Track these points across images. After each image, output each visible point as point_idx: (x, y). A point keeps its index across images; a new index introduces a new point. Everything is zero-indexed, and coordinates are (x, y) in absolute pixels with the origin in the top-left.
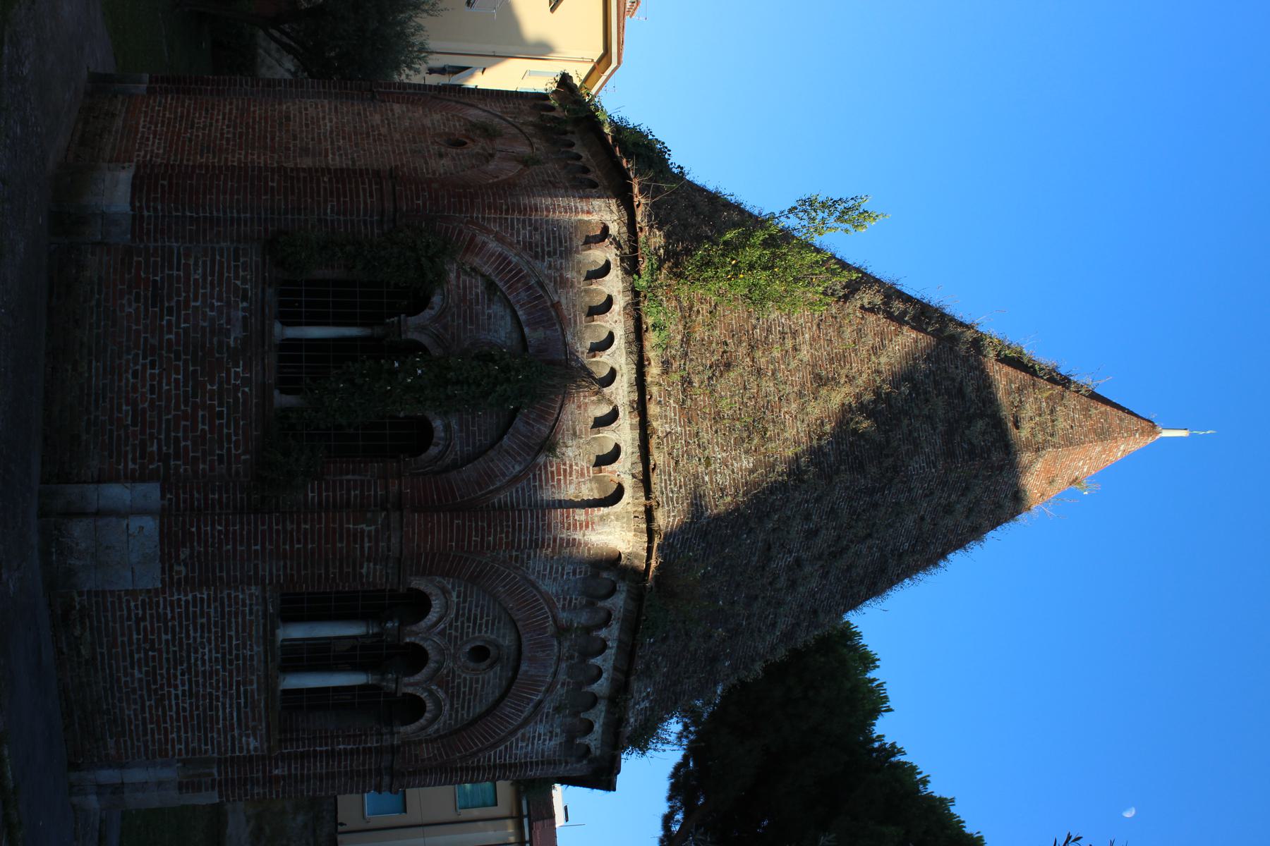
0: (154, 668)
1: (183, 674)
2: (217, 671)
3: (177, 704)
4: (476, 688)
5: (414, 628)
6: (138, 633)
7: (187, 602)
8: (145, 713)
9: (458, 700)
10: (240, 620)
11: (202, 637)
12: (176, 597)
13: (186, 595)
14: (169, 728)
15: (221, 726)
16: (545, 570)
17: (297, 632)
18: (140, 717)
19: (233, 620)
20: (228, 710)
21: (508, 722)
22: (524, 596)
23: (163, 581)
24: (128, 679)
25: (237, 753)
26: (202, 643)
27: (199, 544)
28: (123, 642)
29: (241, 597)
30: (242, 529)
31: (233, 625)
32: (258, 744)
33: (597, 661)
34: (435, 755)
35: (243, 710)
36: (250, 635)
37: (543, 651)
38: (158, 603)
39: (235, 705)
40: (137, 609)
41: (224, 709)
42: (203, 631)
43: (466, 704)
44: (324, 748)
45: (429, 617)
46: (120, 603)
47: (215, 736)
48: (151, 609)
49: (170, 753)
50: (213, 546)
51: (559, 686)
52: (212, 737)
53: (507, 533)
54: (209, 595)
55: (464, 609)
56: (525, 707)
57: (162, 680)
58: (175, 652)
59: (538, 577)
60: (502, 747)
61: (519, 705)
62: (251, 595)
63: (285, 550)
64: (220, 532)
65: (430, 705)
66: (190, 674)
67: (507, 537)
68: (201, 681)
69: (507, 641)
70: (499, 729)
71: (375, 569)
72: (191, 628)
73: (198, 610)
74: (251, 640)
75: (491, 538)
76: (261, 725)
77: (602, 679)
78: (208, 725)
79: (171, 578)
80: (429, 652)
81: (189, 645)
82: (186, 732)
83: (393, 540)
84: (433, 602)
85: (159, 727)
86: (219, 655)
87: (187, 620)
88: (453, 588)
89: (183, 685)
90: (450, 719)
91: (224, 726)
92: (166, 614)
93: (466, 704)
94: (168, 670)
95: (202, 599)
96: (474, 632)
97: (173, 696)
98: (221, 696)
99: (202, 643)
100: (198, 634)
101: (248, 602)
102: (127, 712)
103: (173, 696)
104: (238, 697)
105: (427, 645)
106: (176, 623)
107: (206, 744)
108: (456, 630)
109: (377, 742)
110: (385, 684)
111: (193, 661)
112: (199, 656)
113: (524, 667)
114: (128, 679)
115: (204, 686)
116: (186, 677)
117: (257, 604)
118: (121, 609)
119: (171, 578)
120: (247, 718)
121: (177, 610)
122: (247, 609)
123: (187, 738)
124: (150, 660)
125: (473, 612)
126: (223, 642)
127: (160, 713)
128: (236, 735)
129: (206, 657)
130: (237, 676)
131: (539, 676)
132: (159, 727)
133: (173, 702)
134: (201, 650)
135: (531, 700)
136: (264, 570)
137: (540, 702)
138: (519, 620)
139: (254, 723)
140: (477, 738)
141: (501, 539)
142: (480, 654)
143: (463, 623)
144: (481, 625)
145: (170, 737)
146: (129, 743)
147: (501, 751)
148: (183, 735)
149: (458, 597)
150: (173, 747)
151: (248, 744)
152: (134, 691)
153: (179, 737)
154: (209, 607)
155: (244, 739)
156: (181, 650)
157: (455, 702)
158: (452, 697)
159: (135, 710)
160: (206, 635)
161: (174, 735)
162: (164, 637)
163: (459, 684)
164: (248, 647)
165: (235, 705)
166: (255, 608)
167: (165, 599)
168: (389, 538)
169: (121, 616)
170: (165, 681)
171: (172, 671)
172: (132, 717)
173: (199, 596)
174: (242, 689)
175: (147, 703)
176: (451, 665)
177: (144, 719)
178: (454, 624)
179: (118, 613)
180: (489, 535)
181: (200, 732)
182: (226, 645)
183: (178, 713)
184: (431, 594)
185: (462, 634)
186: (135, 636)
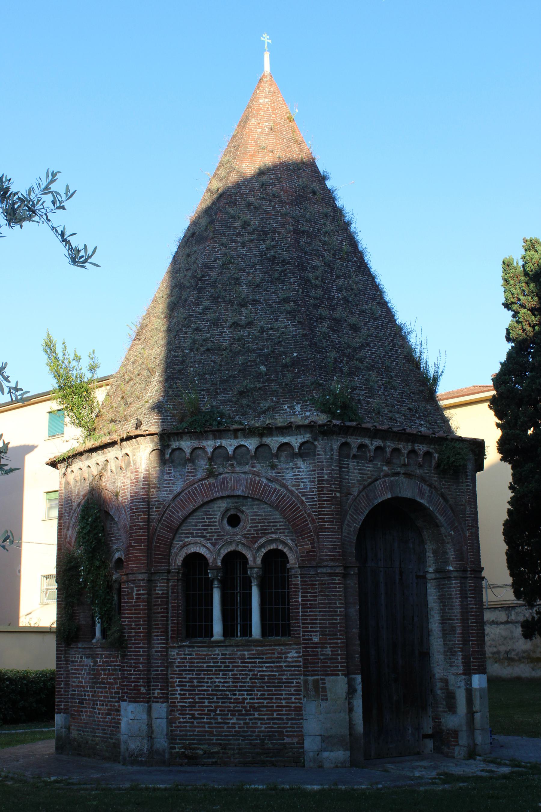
0: (228, 711)
1: (235, 695)
3: (258, 699)
5: (210, 561)
6: (203, 718)
7: (181, 690)
8: (264, 719)
9: (268, 529)
10: (196, 661)
11: (207, 682)
12: (178, 696)
13: (177, 690)
14: (277, 704)
15: (277, 674)
16: (166, 491)
17: (218, 628)
18: (268, 721)
19: (195, 665)
20: (264, 669)
21: (284, 497)
22: (186, 500)
23: (162, 702)
24: (237, 726)
25: (301, 664)
26: (211, 683)
27: (139, 682)
28: (209, 727)
29: (179, 660)
30: (133, 659)
31: (199, 665)
33: (230, 450)
34: (308, 540)
35: (264, 660)
36: (206, 655)
37: (227, 483)
38: (181, 706)
39: (261, 665)
40: (186, 718)
41: (263, 671)
42: (203, 682)
44: (300, 610)
45: (203, 553)
46: (181, 727)
47: (285, 677)
48: (186, 710)
49: (298, 705)
50: (139, 675)
52: (286, 679)
53: (139, 515)
54: (177, 678)
55: (197, 533)
56: (272, 488)
57: (239, 707)
58: (217, 698)
59: (171, 494)
60: (303, 498)
61: (270, 492)
62: (178, 654)
63: (143, 636)
64: (134, 671)
65: (273, 546)
66: (235, 690)
67: (141, 515)
68: (240, 684)
69: (223, 505)
70: (289, 501)
71: (160, 586)
72: (200, 688)
73: (188, 684)
74: (211, 655)
75: (141, 524)
76: (277, 649)
77: (246, 444)
78: (276, 681)
79: (161, 698)
80: (229, 550)
81: (212, 690)
82: (282, 694)
83: (140, 578)
84: (192, 551)
85: (275, 711)
86: (221, 673)
87: (195, 690)
88: (182, 541)
89: (243, 695)
90: (284, 533)
91: (277, 671)
92: (190, 702)
93: (271, 524)
94: (231, 703)
95: (179, 682)
96: (216, 525)
97: (252, 701)
98: (253, 673)
99: (211, 683)
100: (205, 685)
101: (183, 656)
102: (263, 729)
103: (252, 701)
104: (255, 662)
105: (224, 552)
106: (197, 697)
107: (293, 683)
108: (213, 536)
109: (297, 577)
110: (255, 575)
112: (221, 684)
113: (239, 493)
114: (237, 726)
115: (245, 682)
116: (237, 693)
117: (185, 651)
118: (186, 727)
119: (161, 698)
120: (271, 658)
121: (187, 696)
122: (188, 657)
123: (286, 694)
124: (223, 713)
125: (200, 527)
126: (212, 671)
127: (265, 709)
128: (285, 664)
129: (222, 681)
131: (247, 483)
132: (275, 711)
133: (256, 701)
134: (217, 684)
135: (266, 485)
136: (158, 647)
137: (267, 479)
138: (202, 501)
139: (276, 653)
141: (141, 519)
142: (234, 521)
144: (210, 522)
145: (284, 704)
146: (288, 729)
147: (306, 499)
148: (284, 696)
149: (188, 537)
150: (293, 703)
151: (293, 657)
152: (244, 723)
153: (285, 699)
154: (185, 678)
155: (288, 660)
156: (217, 695)
158: (264, 533)
159: (261, 724)
160: (206, 680)
161: (283, 702)
162: (206, 704)
163: (255, 530)
164: (216, 656)
165: (261, 665)
166: (187, 652)
167: (178, 702)
168: (139, 580)
169: (190, 727)
170: (240, 705)
171: (232, 701)
172: (267, 726)
173: (177, 683)
174: (247, 660)
175: (257, 716)
176: (239, 536)
177: (268, 719)
178: (208, 538)
179: (188, 728)
180: (139, 525)
181: (282, 687)
182: (214, 669)
183: (265, 699)
184: (186, 553)
185: (216, 532)
186: (205, 720)
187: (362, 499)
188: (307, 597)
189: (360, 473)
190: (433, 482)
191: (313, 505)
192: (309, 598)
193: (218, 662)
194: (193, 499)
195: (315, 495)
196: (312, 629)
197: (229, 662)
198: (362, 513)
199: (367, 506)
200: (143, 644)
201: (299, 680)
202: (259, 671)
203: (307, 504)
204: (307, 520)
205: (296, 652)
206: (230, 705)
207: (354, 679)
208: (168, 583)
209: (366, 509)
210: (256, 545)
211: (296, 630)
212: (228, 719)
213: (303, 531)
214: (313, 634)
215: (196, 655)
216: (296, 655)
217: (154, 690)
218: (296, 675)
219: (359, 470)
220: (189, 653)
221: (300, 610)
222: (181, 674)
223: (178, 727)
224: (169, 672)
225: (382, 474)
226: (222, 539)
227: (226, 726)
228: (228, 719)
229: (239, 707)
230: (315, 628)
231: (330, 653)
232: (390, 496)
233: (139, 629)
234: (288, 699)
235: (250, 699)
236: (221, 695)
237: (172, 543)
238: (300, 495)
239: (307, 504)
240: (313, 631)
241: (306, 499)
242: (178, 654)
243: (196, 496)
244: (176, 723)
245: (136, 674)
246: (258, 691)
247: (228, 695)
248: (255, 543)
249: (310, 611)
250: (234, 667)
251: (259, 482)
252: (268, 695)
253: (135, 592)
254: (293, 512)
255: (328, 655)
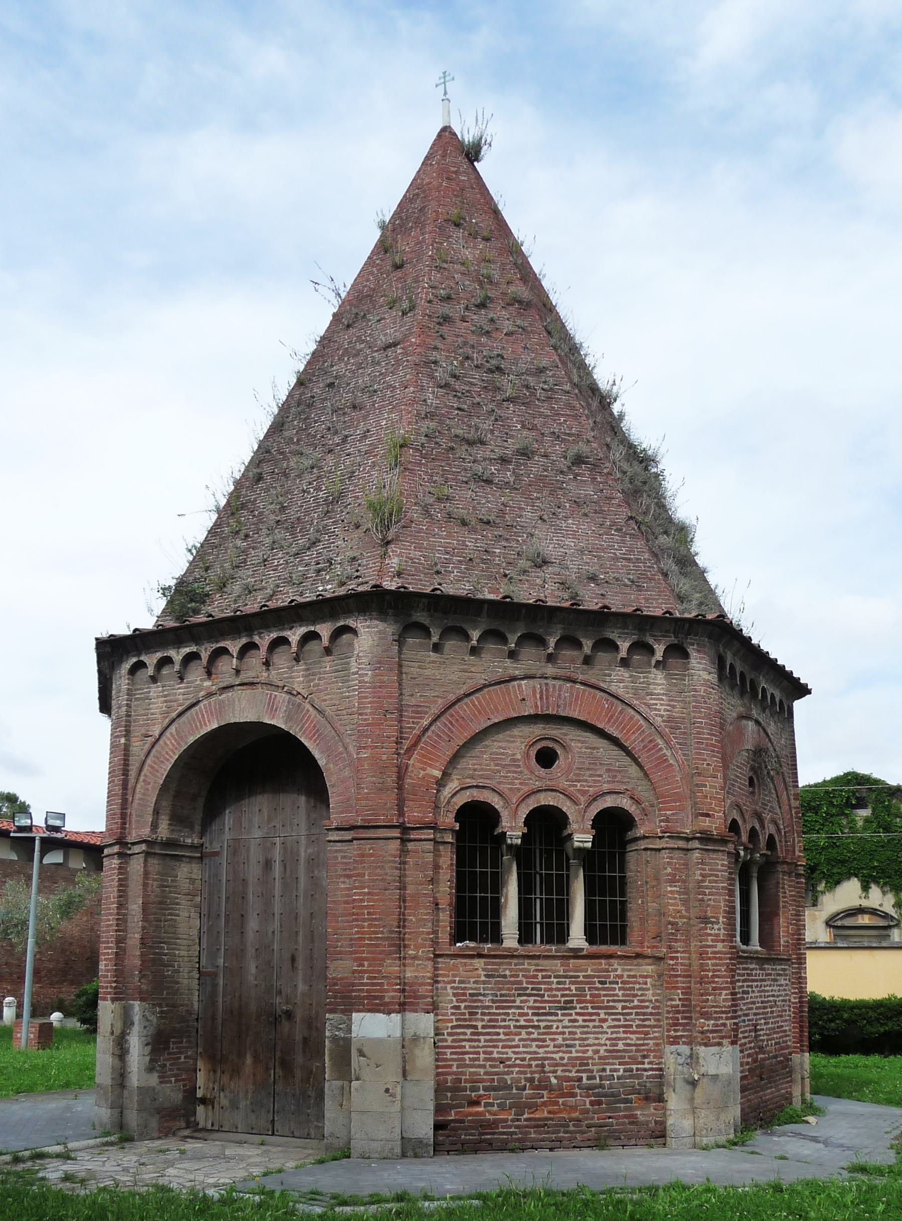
187: (169, 739)
189: (166, 702)
190: (295, 686)
198: (168, 760)
199: (176, 749)
207: (132, 1006)
209: (174, 753)
219: (165, 696)
225: (202, 693)
232: (215, 726)
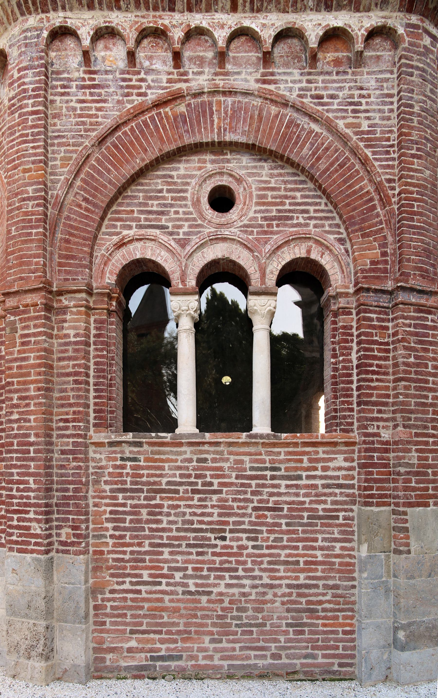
0: (209, 569)
1: (224, 539)
2: (220, 500)
3: (268, 547)
4: (273, 197)
10: (145, 472)
11: (169, 514)
13: (107, 529)
14: (306, 559)
21: (327, 149)
23: (76, 553)
25: (355, 482)
29: (111, 470)
30: (16, 467)
32: (341, 457)
38: (114, 560)
42: (160, 513)
43: (298, 208)
49: (348, 560)
51: (272, 87)
54: (107, 505)
60: (368, 152)
70: (337, 159)
73: (129, 518)
81: (178, 530)
82: (316, 540)
86: (196, 496)
88: (118, 234)
95: (111, 512)
101: (119, 463)
104: (264, 477)
107: (337, 517)
109: (350, 313)
111: (204, 527)
112: (195, 518)
115: (244, 515)
116: (228, 535)
121: (128, 540)
122: (129, 464)
126: (177, 492)
129: (199, 511)
130: (230, 477)
134: (187, 517)
138: (160, 150)
140: (350, 187)
143: (170, 220)
145: (320, 559)
147: (374, 153)
151: (340, 469)
153: (321, 548)
154: (124, 505)
157: (295, 222)
160: (165, 510)
161: (318, 553)
162: (166, 556)
167: (109, 552)
170: (233, 559)
173: (108, 516)
174: (249, 473)
178: (170, 229)
182: (181, 489)
188: (372, 350)
191: (388, 166)
192: (376, 353)
193: (190, 476)
194: (141, 145)
195: (392, 146)
196: (380, 416)
197: (212, 476)
200: (37, 435)
201: (351, 514)
202: (272, 494)
203: (376, 164)
204: (372, 200)
205: (346, 460)
206: (215, 558)
208: (88, 315)
210: (268, 247)
211: (345, 417)
212: (208, 585)
213: (364, 220)
214: (381, 424)
215: (146, 460)
216: (347, 464)
217: (59, 527)
218: (345, 503)
220: (132, 456)
221: (355, 378)
222: (116, 498)
223: (109, 600)
224: (91, 493)
226: (200, 232)
227: (204, 599)
228: (208, 585)
229: (231, 562)
230: (385, 412)
231: (416, 462)
233: (28, 405)
234: (327, 548)
235: (254, 547)
236: (194, 539)
237: (96, 237)
238: (361, 144)
239: (376, 164)
240: (382, 419)
241: (374, 153)
242: (109, 459)
243: (146, 139)
244: (103, 593)
245: (22, 497)
246: (269, 532)
247: (209, 539)
248: (266, 243)
249: (377, 380)
250: (220, 484)
251: (277, 116)
252: (289, 540)
253: (20, 332)
254: (345, 182)
255: (412, 465)
